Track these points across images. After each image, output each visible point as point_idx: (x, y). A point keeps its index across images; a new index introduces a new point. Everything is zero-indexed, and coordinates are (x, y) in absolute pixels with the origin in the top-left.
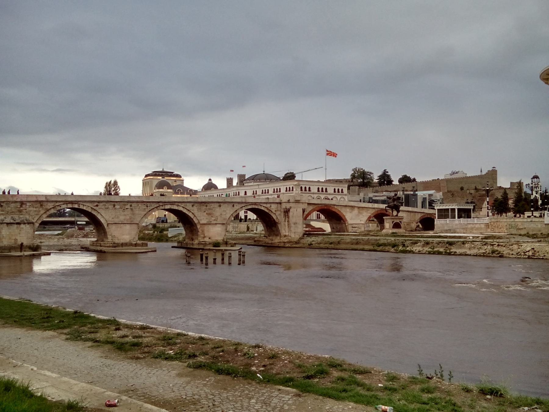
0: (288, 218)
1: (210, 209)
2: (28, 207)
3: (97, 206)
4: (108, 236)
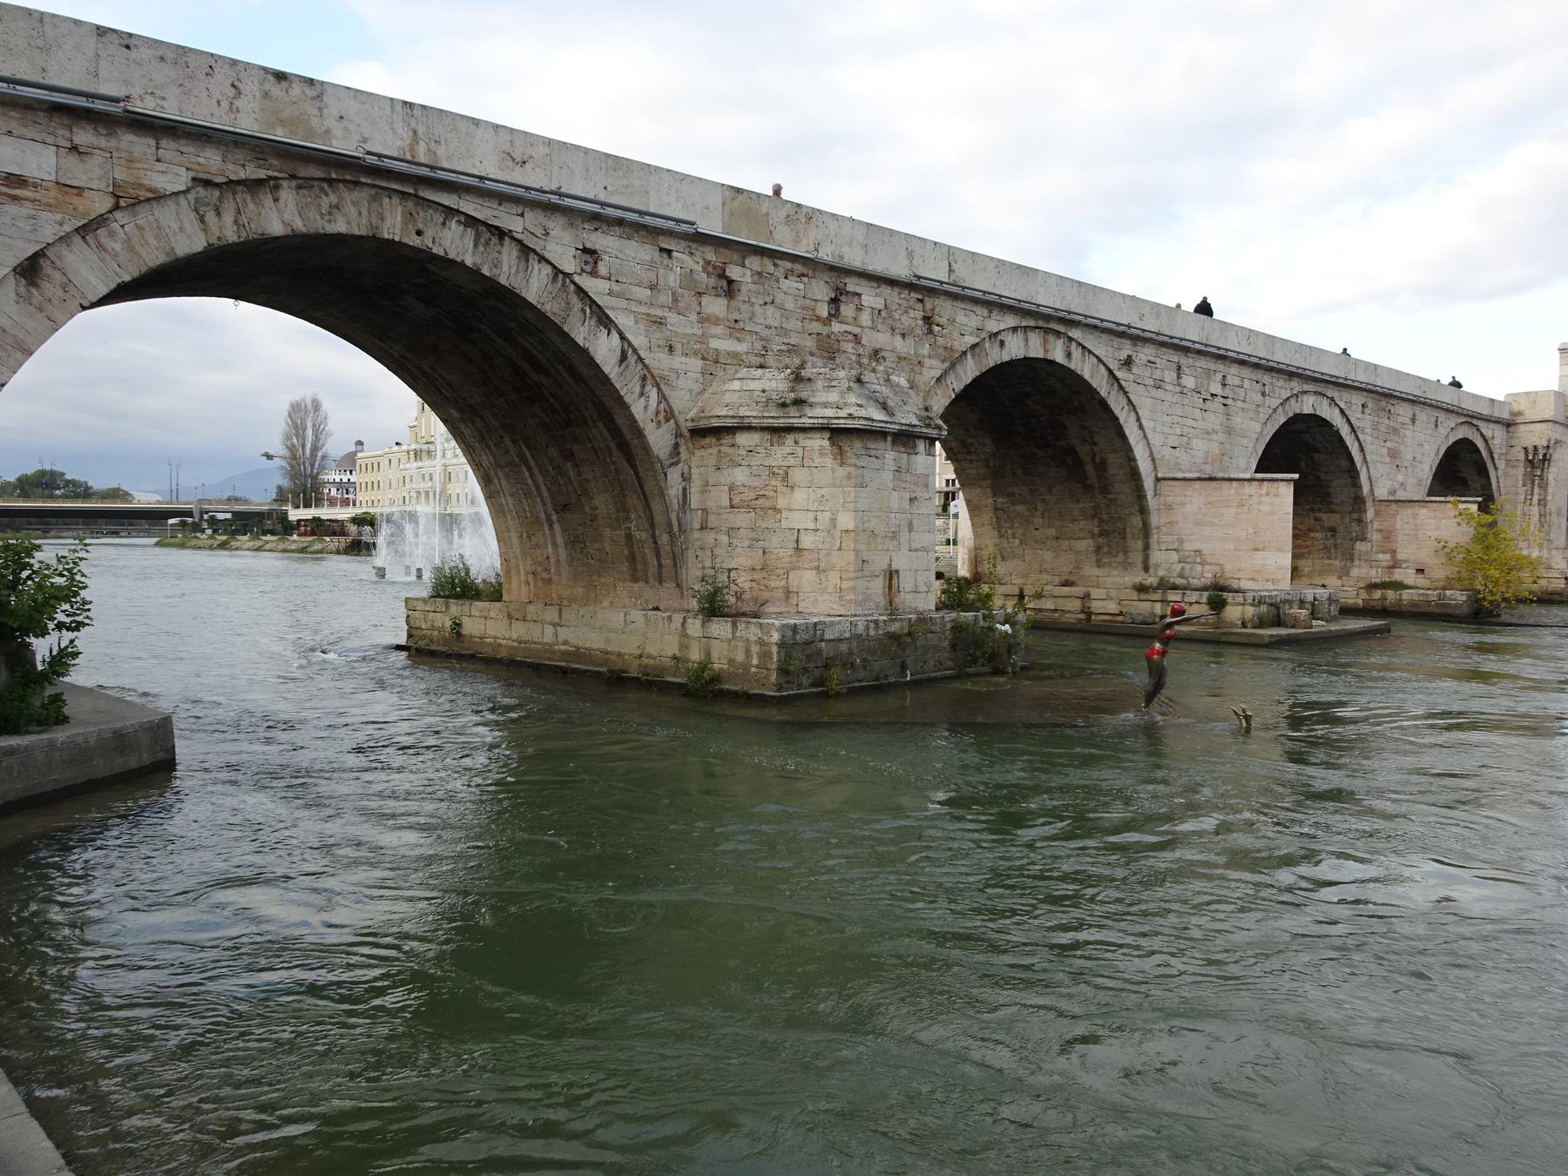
0: (1544, 486)
1: (1395, 430)
2: (865, 318)
3: (1128, 363)
4: (1157, 556)
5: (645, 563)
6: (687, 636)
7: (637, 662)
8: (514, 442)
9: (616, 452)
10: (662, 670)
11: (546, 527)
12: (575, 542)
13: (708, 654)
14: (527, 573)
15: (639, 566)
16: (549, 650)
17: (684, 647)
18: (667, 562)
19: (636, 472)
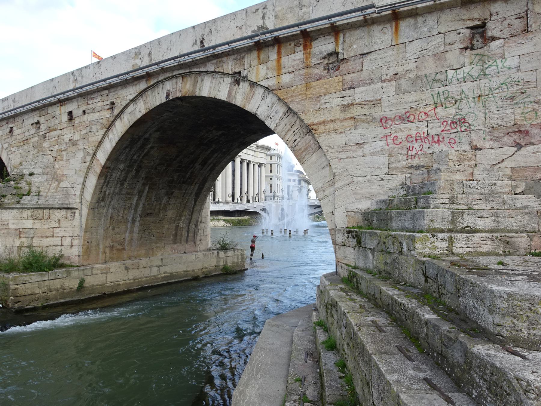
5: (181, 236)
6: (219, 258)
7: (201, 271)
8: (144, 184)
9: (193, 195)
10: (210, 271)
11: (129, 224)
12: (145, 230)
13: (226, 262)
14: (105, 247)
15: (178, 237)
16: (156, 278)
17: (218, 262)
18: (191, 235)
19: (195, 202)
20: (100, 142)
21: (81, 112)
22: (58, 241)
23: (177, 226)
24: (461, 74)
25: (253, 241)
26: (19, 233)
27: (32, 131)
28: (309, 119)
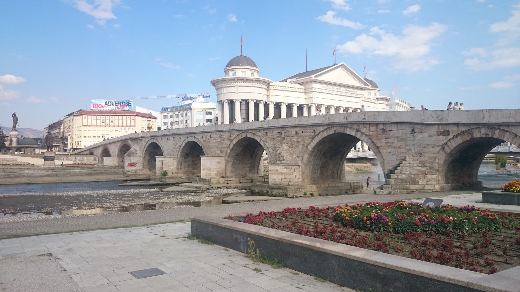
18: (339, 175)
20: (309, 143)
21: (301, 132)
22: (294, 176)
23: (333, 172)
24: (410, 139)
25: (368, 180)
26: (282, 174)
27: (278, 136)
28: (378, 145)
